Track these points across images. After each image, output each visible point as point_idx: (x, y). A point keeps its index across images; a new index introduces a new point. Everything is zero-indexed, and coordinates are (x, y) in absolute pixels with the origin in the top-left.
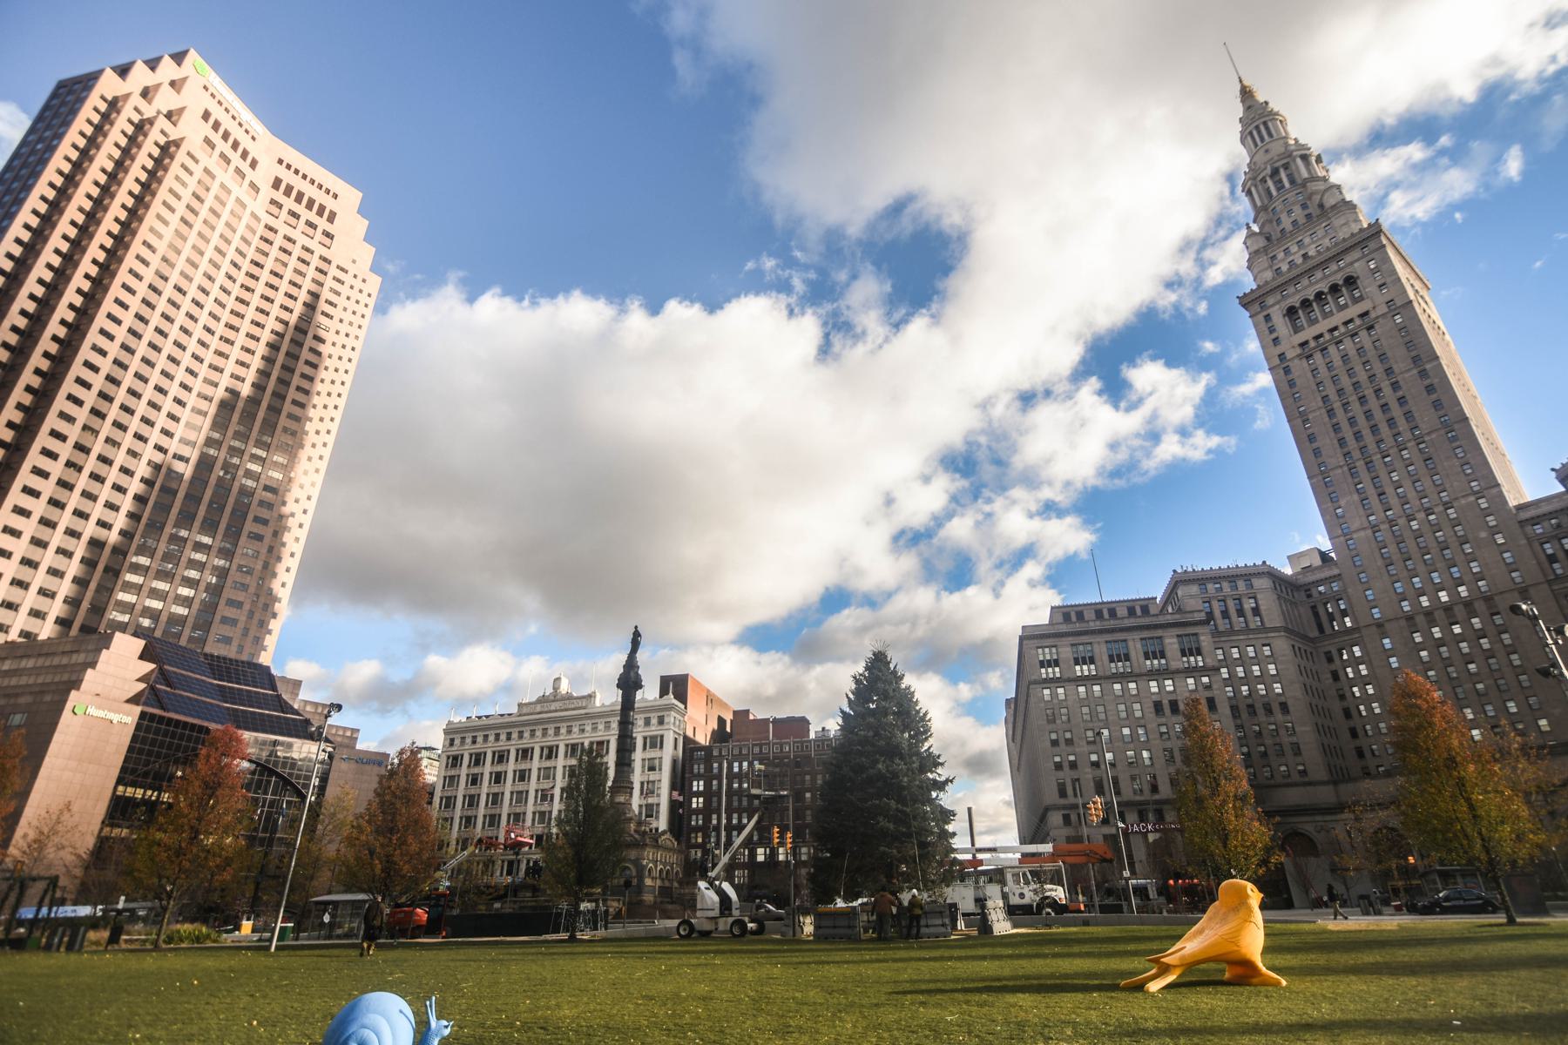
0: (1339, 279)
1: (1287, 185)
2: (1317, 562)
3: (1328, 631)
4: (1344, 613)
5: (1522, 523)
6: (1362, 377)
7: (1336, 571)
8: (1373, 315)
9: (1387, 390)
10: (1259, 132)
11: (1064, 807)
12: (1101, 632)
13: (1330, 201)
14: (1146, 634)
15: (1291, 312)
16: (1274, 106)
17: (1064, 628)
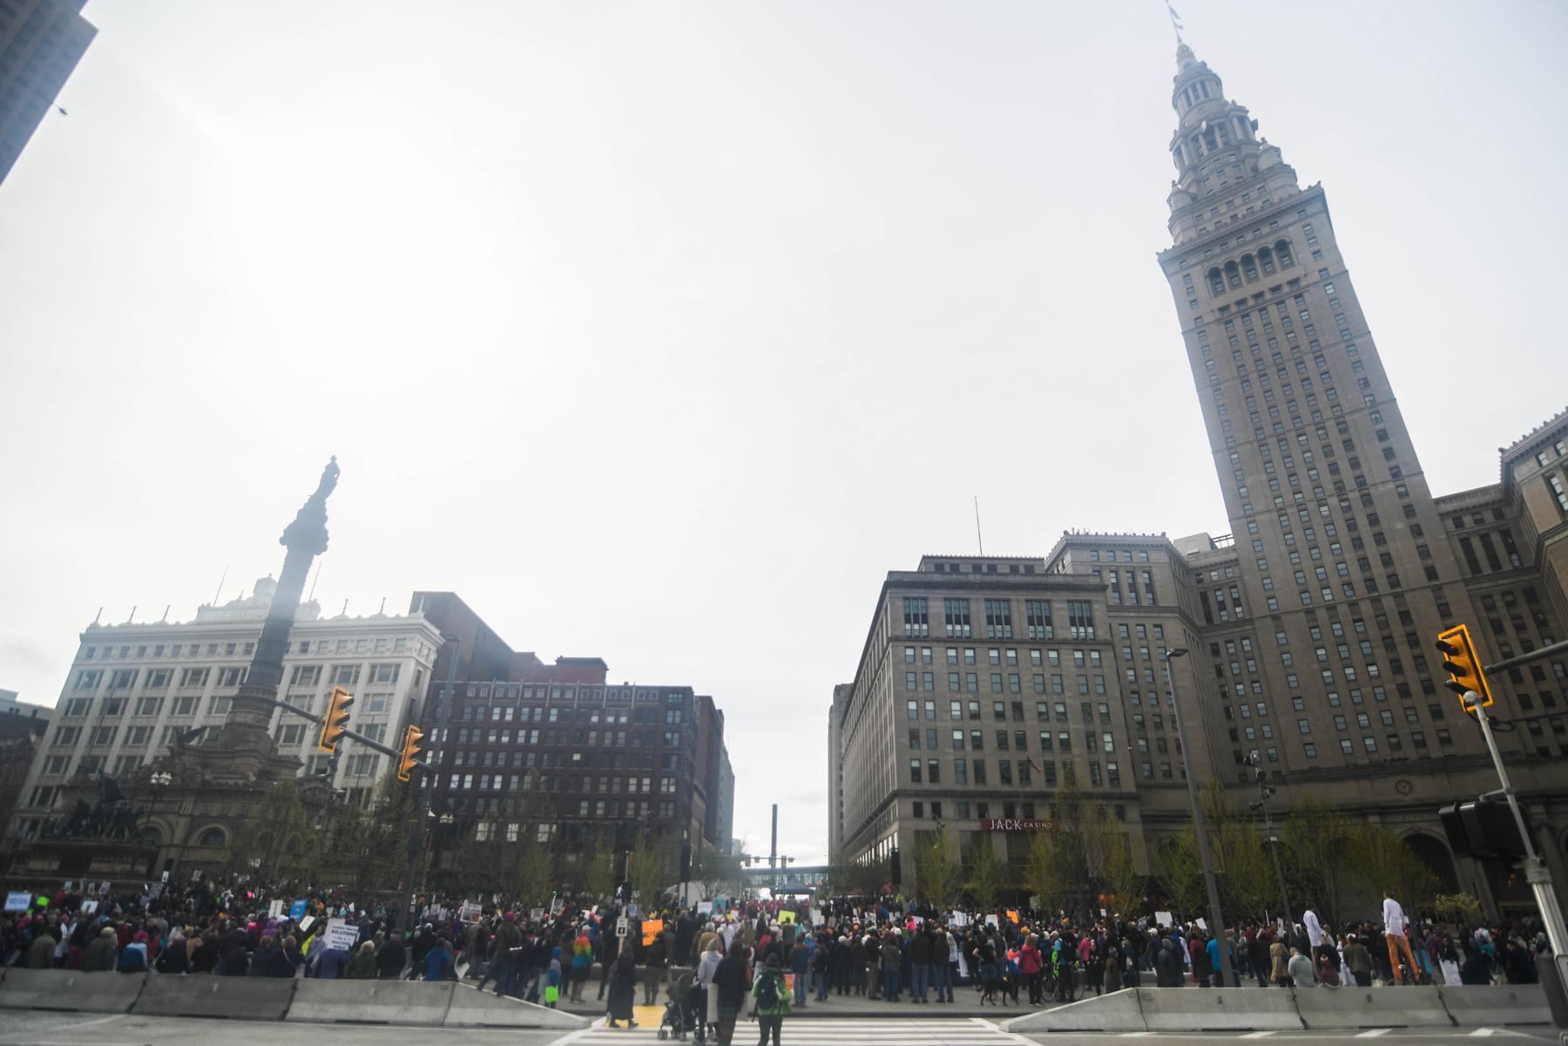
0: (1270, 242)
1: (1220, 145)
2: (1208, 548)
3: (1216, 622)
4: (1237, 602)
5: (1443, 516)
6: (1285, 348)
7: (1233, 556)
8: (1303, 283)
9: (1310, 363)
10: (1195, 90)
11: (917, 794)
12: (982, 586)
13: (1264, 164)
14: (1032, 595)
15: (1214, 274)
16: (1213, 67)
17: (938, 578)
